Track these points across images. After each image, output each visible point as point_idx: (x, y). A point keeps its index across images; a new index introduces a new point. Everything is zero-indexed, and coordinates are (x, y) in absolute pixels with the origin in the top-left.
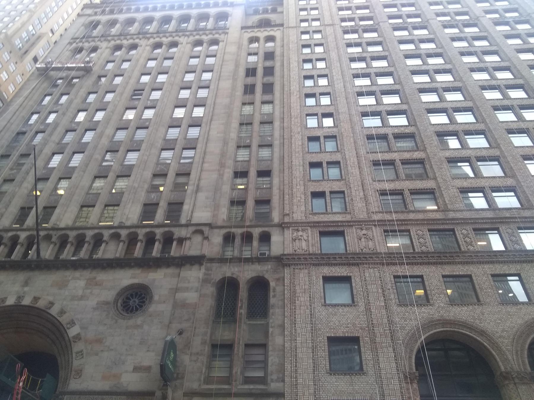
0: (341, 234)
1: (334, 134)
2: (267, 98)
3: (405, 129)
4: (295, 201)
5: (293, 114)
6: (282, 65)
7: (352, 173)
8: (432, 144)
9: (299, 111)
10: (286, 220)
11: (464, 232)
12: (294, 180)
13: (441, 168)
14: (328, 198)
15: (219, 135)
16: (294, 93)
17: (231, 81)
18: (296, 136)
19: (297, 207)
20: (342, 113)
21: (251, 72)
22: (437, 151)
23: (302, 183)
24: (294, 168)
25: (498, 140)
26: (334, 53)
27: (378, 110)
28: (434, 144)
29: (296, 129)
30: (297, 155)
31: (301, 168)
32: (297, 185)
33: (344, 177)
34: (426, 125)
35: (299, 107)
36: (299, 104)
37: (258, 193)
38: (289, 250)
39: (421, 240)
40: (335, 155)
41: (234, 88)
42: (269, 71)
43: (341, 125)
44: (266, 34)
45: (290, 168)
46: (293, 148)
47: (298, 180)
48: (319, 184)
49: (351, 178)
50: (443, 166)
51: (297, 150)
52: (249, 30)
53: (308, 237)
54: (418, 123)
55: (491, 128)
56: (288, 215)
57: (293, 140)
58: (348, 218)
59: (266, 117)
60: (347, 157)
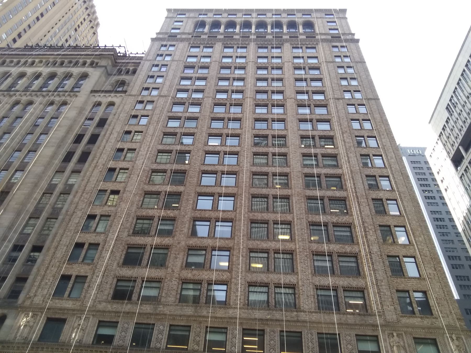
0: (63, 321)
1: (110, 214)
2: (78, 167)
3: (171, 212)
4: (43, 283)
5: (87, 188)
6: (105, 135)
7: (103, 257)
8: (183, 231)
9: (93, 186)
10: (28, 303)
11: (161, 327)
12: (53, 261)
13: (176, 258)
14: (71, 282)
15: (16, 206)
16: (98, 166)
17: (53, 149)
18: (78, 212)
19: (42, 290)
20: (128, 191)
21: (79, 139)
22: (182, 239)
23: (58, 264)
24: (59, 248)
25: (236, 232)
26: (152, 126)
27: (160, 190)
28: (183, 232)
29: (82, 205)
30: (68, 233)
31: (65, 248)
32: (52, 267)
33: (94, 261)
34: (188, 210)
35: (95, 182)
36: (97, 179)
37: (22, 269)
38: (11, 337)
39: (123, 333)
40: (100, 236)
41: (53, 157)
42: (94, 139)
43: (120, 205)
44: (110, 99)
45: (56, 248)
46: (69, 225)
47: (56, 261)
48: (71, 266)
49: (100, 263)
50: (178, 256)
51: (71, 228)
52: (96, 95)
53: (34, 323)
54: (182, 208)
55: (237, 219)
56: (30, 298)
57: (73, 216)
58: (77, 305)
59: (67, 188)
60: (108, 239)
